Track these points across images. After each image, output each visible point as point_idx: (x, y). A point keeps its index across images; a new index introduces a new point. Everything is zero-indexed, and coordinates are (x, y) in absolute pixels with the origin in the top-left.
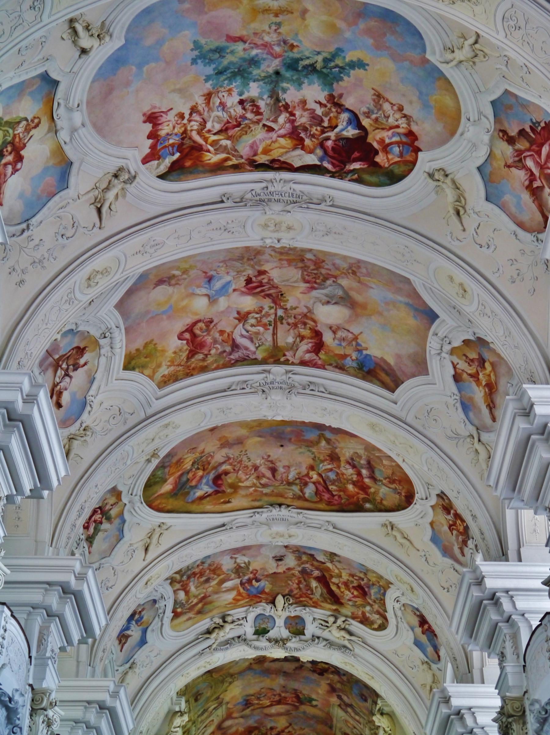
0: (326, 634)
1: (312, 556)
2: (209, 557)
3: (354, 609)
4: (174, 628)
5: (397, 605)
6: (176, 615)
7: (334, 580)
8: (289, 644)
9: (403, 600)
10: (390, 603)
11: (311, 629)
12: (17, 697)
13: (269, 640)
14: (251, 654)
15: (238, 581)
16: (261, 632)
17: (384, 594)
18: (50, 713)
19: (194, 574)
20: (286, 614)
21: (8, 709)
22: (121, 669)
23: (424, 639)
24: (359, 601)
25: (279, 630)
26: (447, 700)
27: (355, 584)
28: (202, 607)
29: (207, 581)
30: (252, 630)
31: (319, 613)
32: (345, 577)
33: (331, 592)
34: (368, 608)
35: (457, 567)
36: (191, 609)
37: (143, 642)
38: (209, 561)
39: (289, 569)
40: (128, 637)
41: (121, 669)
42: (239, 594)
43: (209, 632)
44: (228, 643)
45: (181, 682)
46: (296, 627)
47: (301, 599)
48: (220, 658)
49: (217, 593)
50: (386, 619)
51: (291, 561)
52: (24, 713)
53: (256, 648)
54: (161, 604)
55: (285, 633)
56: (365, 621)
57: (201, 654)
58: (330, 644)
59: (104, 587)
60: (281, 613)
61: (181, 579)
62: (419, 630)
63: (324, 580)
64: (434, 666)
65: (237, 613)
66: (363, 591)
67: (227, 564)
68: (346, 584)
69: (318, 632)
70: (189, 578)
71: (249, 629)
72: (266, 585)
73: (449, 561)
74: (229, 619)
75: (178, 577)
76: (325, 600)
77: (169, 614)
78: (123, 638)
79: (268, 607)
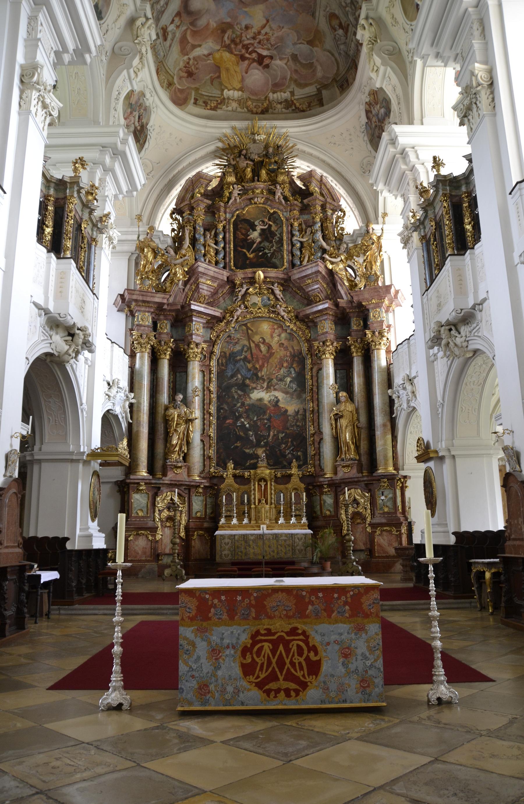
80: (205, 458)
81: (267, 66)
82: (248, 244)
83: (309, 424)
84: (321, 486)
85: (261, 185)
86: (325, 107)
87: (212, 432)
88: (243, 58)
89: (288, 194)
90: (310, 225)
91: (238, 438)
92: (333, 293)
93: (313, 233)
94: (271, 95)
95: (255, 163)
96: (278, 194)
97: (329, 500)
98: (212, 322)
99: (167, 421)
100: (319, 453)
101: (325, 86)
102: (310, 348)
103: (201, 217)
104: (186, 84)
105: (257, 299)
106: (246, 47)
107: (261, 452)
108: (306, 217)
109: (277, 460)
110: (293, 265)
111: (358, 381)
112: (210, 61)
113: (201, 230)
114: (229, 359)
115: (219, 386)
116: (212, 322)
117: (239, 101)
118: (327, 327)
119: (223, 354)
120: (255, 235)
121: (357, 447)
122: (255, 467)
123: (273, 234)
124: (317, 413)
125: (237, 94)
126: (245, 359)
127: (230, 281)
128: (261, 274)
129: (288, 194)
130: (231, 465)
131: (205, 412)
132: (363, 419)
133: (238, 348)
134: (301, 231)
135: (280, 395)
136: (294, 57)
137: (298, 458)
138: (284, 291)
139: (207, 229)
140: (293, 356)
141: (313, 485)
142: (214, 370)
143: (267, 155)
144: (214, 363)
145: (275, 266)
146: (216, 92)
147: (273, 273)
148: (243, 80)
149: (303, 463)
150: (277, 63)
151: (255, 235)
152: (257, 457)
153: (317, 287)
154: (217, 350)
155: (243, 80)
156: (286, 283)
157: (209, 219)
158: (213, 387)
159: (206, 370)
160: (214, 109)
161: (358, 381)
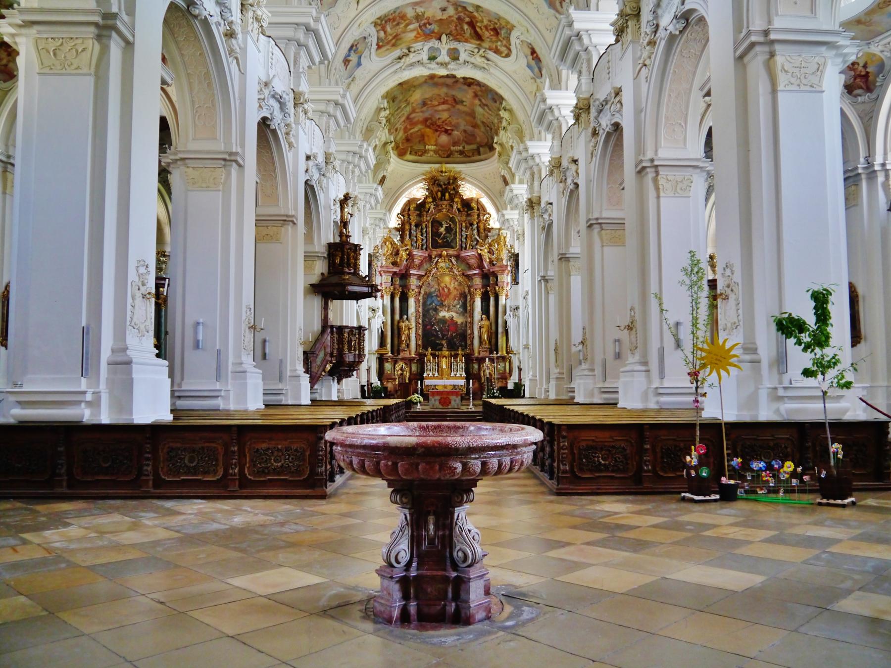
0: (472, 60)
1: (465, 8)
2: (398, 8)
3: (491, 44)
4: (377, 55)
5: (518, 41)
6: (379, 47)
7: (478, 24)
8: (449, 66)
9: (522, 38)
10: (513, 40)
11: (463, 56)
12: (284, 96)
13: (437, 64)
14: (426, 72)
15: (417, 25)
16: (432, 58)
17: (510, 34)
18: (306, 106)
19: (389, 20)
20: (447, 47)
21: (280, 102)
22: (347, 81)
23: (533, 63)
24: (494, 38)
25: (444, 57)
26: (544, 100)
27: (492, 27)
28: (395, 42)
29: (398, 24)
30: (427, 57)
31: (469, 46)
32: (486, 22)
33: (476, 33)
34: (499, 43)
35: (557, 15)
36: (388, 43)
37: (359, 64)
38: (398, 11)
39: (450, 17)
40: (349, 61)
41: (347, 81)
42: (418, 33)
43: (400, 58)
44: (412, 65)
45: (384, 90)
46: (454, 55)
47: (457, 36)
48: (407, 75)
49: (404, 32)
50: (510, 50)
51: (451, 11)
52: (290, 105)
53: (429, 68)
54: (369, 39)
55: (447, 59)
56: (497, 51)
57: (395, 72)
58: (475, 66)
59: (332, 28)
60: (445, 46)
61: (381, 23)
62: (530, 57)
63: (472, 24)
64: (538, 80)
65: (417, 46)
66: (496, 32)
67: (410, 13)
68: (486, 27)
69: (468, 59)
70: (386, 22)
71: (424, 56)
72: (435, 27)
73: (552, 11)
74: (412, 50)
75: (379, 21)
76: (472, 38)
77: (374, 46)
78: (346, 62)
79: (437, 42)
80: (417, 345)
81: (450, 134)
82: (438, 235)
83: (468, 329)
84: (472, 360)
85: (445, 203)
86: (482, 157)
87: (420, 332)
88: (437, 131)
89: (459, 206)
90: (472, 225)
91: (433, 335)
92: (480, 266)
93: (473, 230)
94: (452, 148)
95: (443, 189)
96: (455, 207)
97: (476, 366)
98: (420, 277)
99: (399, 329)
100: (472, 343)
101: (482, 146)
102: (469, 291)
103: (414, 219)
104: (406, 145)
105: (442, 265)
106: (439, 126)
107: (444, 342)
108: (469, 218)
109: (452, 346)
110: (462, 247)
111: (492, 309)
112: (419, 133)
113: (414, 228)
114: (428, 295)
115: (423, 309)
116: (420, 277)
117: (435, 152)
118: (478, 281)
119: (426, 293)
120: (442, 230)
121: (490, 342)
122: (441, 350)
123: (452, 230)
124: (472, 323)
125: (433, 148)
126: (437, 296)
127: (430, 256)
128: (445, 253)
129: (459, 206)
130: (430, 349)
131: (417, 323)
132: (494, 328)
133: (433, 290)
134: (467, 228)
135: (454, 314)
136: (465, 131)
137: (462, 346)
138: (457, 261)
139: (417, 226)
140: (461, 294)
141: (469, 360)
142: (421, 301)
143: (449, 183)
144: (421, 298)
145: (452, 248)
146: (422, 147)
147: (451, 252)
148: (436, 140)
149: (464, 348)
150: (456, 133)
151: (442, 230)
152: (443, 345)
153: (473, 261)
154: (423, 291)
155: (436, 140)
156: (457, 257)
157: (418, 219)
158: (421, 310)
159: (417, 301)
160: (420, 156)
161: (492, 309)
